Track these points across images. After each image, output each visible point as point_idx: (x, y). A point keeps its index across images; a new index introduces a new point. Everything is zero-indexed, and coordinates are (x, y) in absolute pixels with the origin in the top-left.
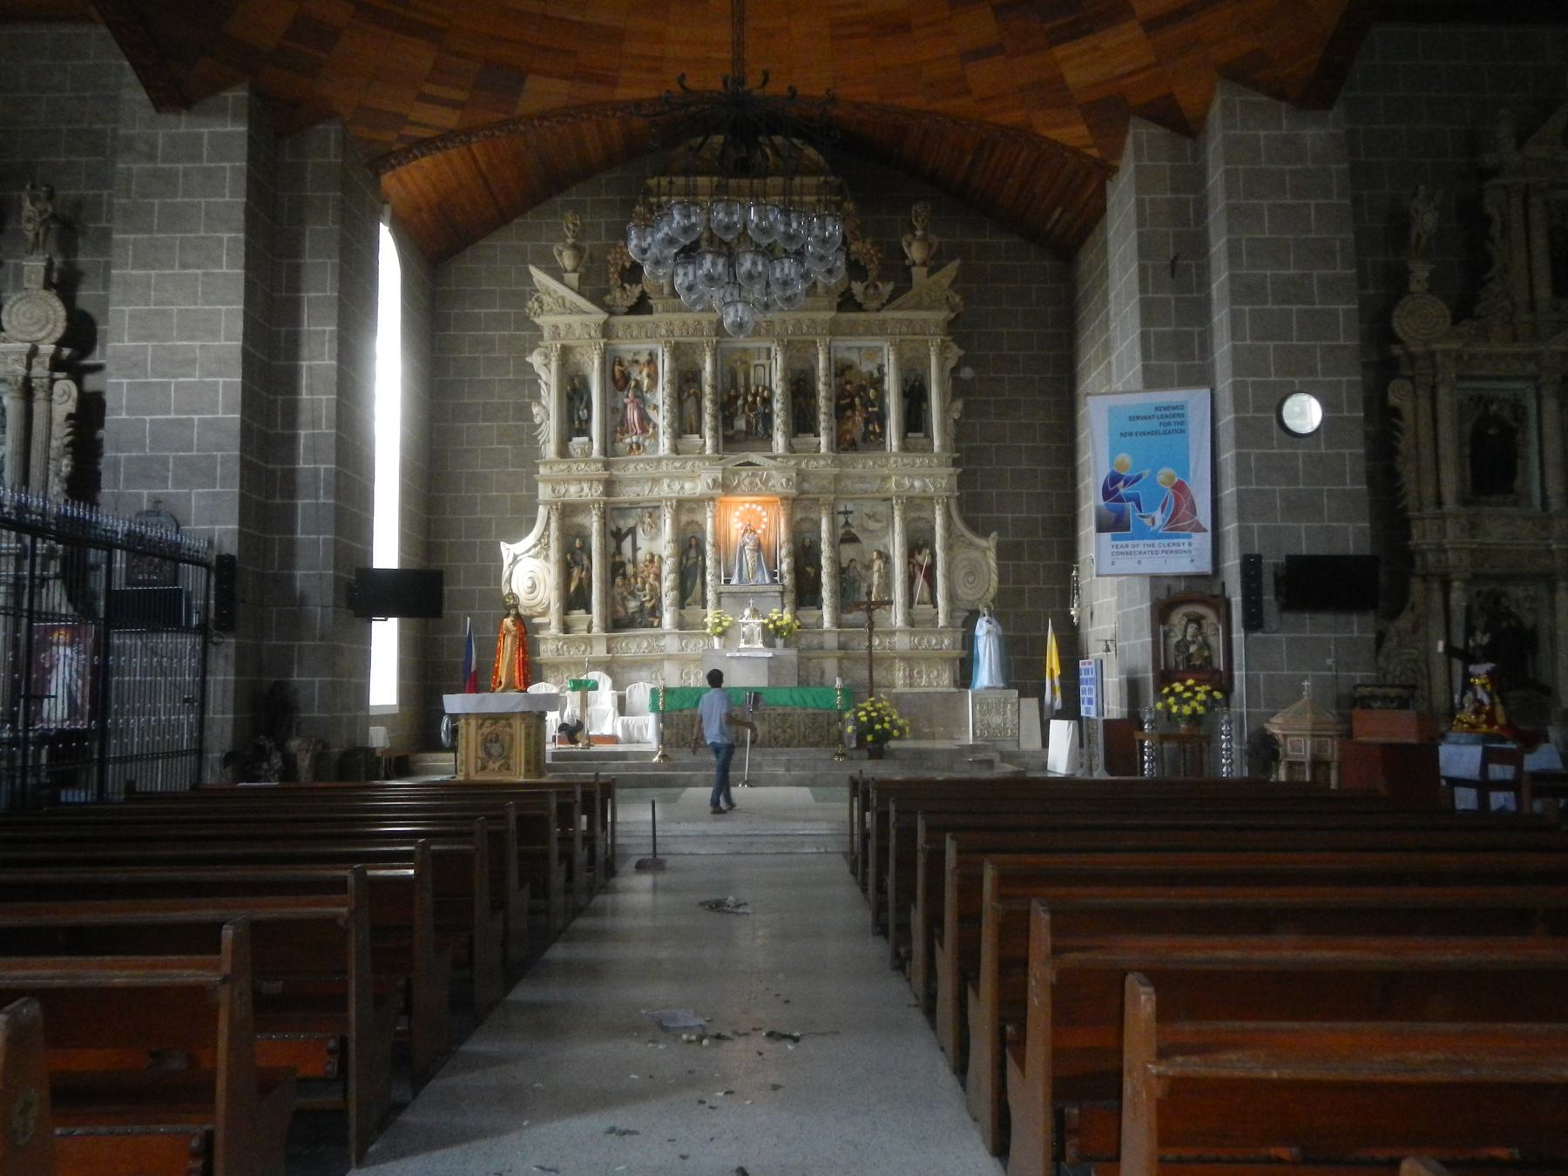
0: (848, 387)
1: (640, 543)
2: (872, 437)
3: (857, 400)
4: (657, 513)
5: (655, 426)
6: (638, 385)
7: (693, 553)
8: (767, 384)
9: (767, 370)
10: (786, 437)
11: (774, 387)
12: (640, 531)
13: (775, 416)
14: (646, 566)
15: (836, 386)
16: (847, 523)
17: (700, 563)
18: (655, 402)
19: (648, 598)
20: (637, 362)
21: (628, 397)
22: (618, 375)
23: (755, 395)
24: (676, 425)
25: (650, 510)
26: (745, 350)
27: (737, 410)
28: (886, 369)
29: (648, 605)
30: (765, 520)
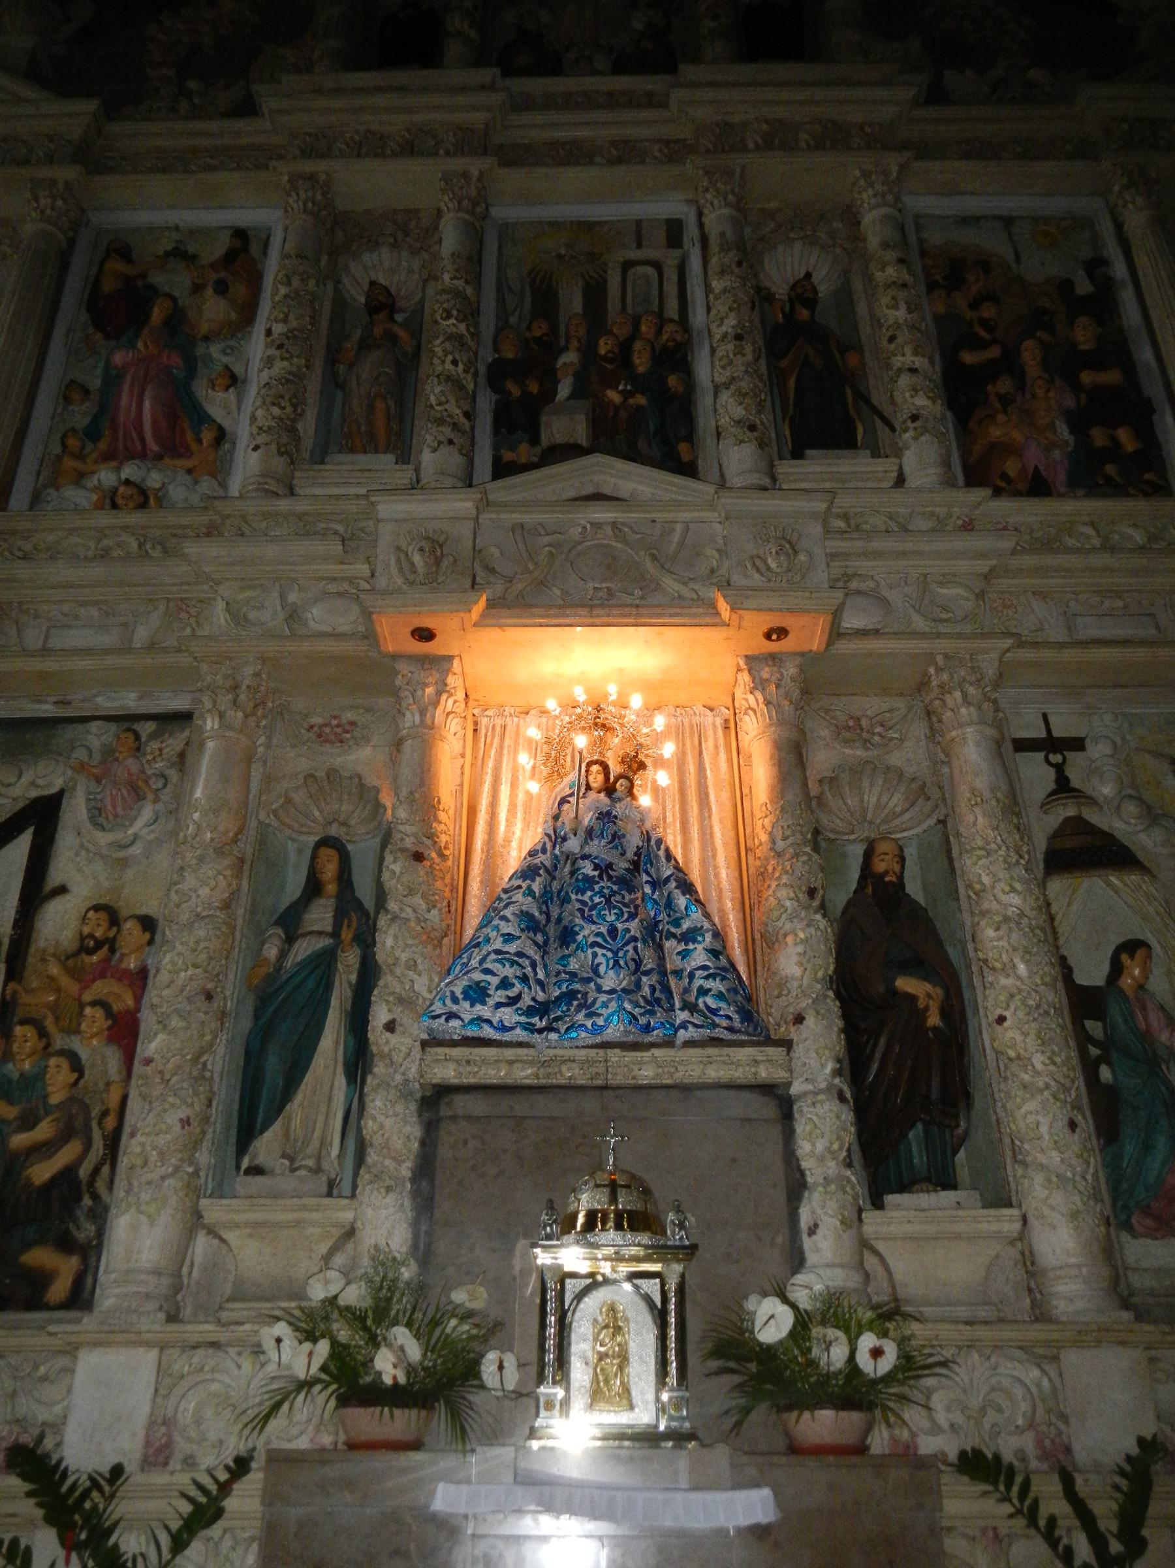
0: (988, 311)
1: (62, 868)
2: (1110, 469)
3: (1030, 354)
4: (174, 743)
5: (221, 435)
6: (176, 321)
7: (320, 915)
8: (672, 309)
9: (671, 275)
10: (762, 445)
11: (698, 317)
12: (75, 811)
13: (704, 401)
14: (74, 973)
15: (937, 318)
16: (1063, 786)
17: (349, 960)
18: (238, 369)
19: (44, 1130)
20: (190, 259)
21: (133, 346)
22: (108, 286)
23: (625, 348)
24: (308, 427)
25: (148, 727)
26: (588, 227)
27: (550, 379)
28: (1119, 269)
29: (42, 1172)
30: (668, 749)
